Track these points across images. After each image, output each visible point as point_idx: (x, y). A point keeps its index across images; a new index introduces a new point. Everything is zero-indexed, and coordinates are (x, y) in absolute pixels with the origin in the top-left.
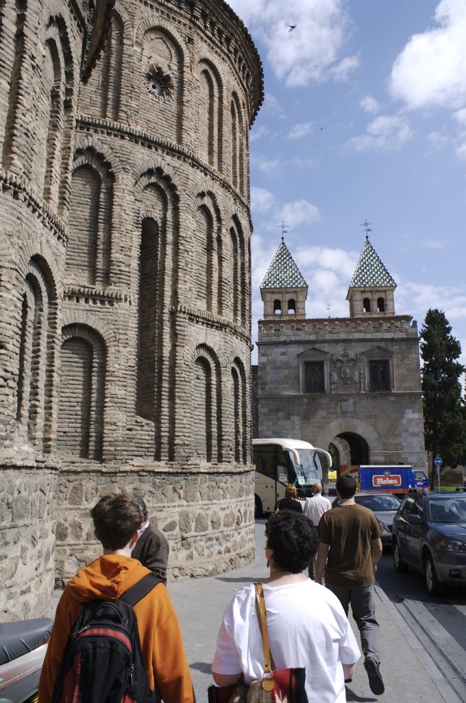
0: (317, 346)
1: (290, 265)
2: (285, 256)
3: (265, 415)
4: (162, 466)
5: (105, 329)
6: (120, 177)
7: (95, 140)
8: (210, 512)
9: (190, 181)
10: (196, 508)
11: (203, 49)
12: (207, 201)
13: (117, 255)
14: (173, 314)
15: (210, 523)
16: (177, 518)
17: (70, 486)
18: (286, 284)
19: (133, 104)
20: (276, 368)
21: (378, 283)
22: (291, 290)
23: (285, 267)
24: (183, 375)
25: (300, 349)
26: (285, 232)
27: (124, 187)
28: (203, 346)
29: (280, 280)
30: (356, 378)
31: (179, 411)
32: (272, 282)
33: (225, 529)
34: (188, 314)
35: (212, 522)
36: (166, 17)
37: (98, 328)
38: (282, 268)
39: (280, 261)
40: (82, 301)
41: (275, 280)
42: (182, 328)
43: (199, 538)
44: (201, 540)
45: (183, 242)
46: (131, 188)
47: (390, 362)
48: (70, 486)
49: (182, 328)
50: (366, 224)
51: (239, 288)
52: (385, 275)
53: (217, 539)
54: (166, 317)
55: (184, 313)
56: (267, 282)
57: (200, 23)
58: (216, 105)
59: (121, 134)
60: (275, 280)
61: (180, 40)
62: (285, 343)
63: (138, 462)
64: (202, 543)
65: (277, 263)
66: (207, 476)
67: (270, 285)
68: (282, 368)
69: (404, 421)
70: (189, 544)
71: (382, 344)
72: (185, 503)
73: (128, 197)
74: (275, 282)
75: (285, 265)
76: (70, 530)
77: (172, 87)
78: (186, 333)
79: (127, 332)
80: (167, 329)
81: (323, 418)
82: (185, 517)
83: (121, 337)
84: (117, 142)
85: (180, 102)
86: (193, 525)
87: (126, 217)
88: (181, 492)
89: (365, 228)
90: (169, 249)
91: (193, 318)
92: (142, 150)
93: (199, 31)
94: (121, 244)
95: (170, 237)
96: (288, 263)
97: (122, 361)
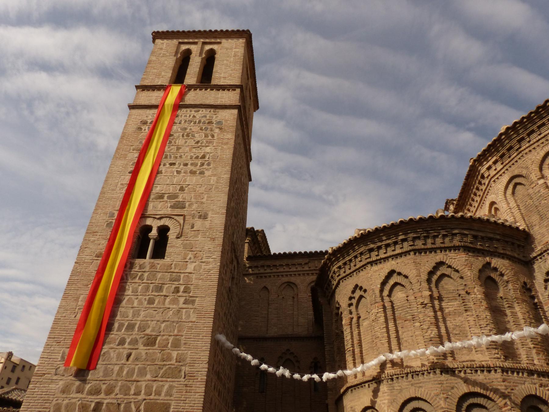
36: (547, 143)
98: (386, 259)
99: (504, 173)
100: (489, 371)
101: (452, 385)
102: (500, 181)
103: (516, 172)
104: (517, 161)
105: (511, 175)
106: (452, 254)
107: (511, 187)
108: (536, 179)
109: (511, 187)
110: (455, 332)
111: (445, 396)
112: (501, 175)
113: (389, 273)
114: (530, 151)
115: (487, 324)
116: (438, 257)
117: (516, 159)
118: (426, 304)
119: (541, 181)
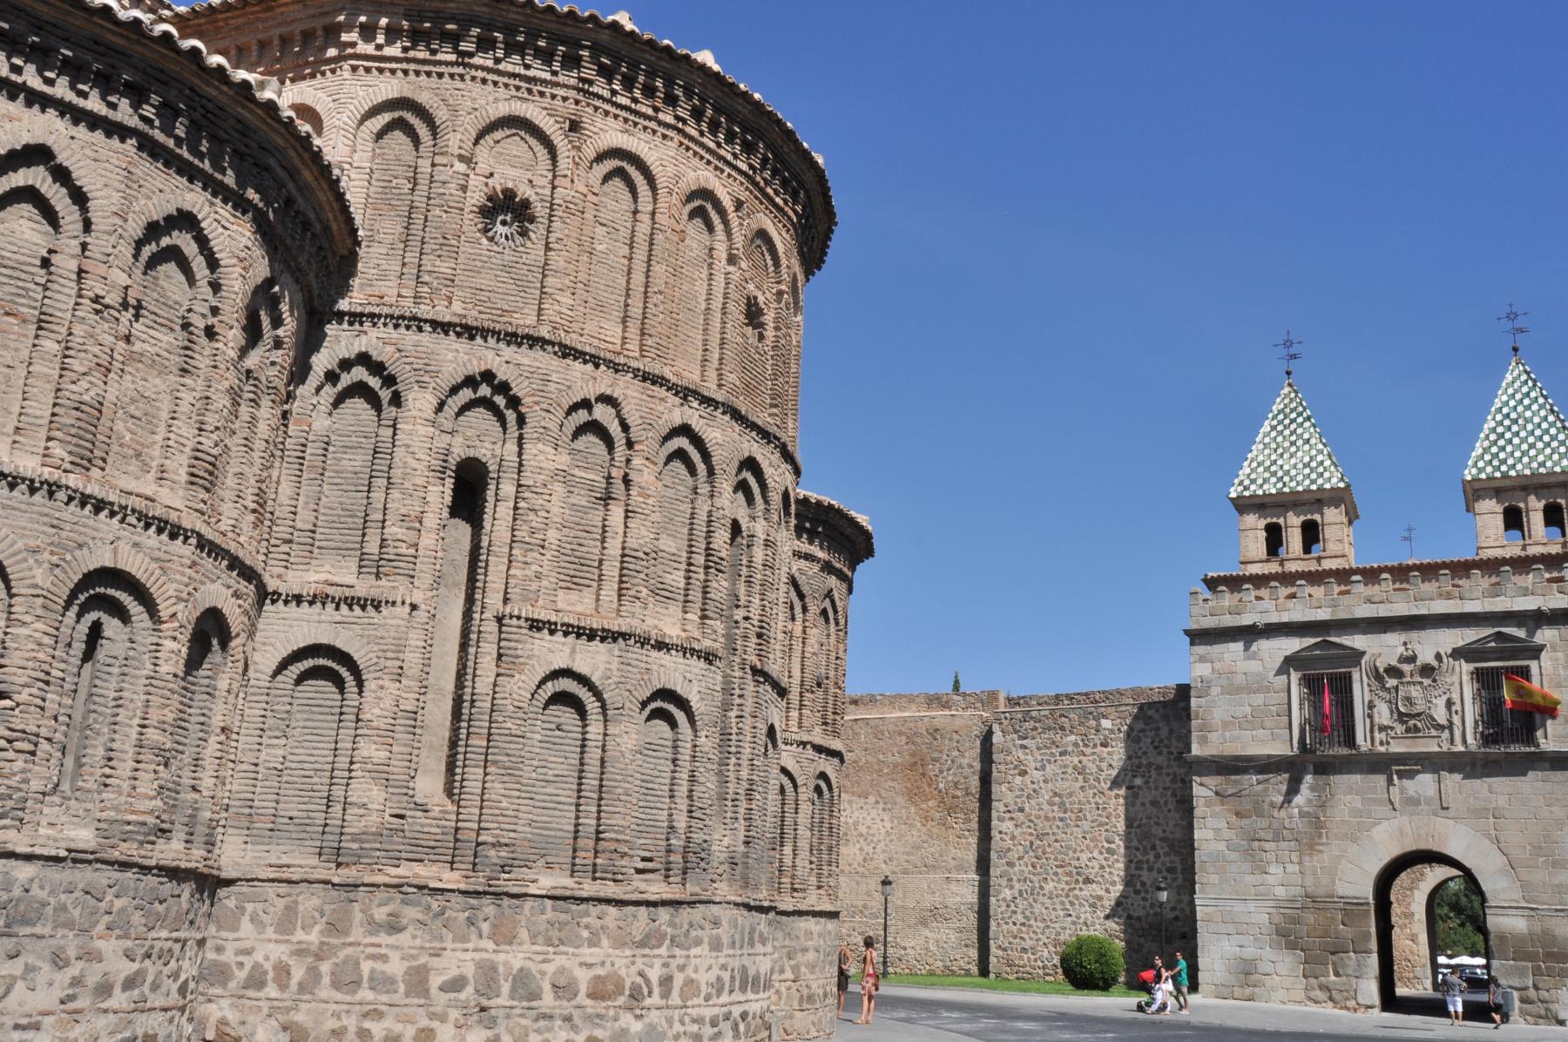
1: (1306, 436)
2: (1293, 415)
4: (451, 879)
5: (363, 652)
6: (410, 398)
7: (371, 340)
8: (550, 969)
10: (514, 958)
11: (609, 133)
12: (602, 413)
13: (394, 529)
15: (547, 987)
16: (469, 971)
17: (281, 903)
18: (1293, 484)
19: (444, 267)
21: (1543, 464)
22: (1306, 497)
23: (1293, 443)
24: (509, 725)
25: (1293, 645)
26: (1293, 357)
27: (414, 413)
29: (1280, 474)
30: (1441, 716)
31: (496, 788)
32: (1260, 481)
33: (589, 1002)
34: (527, 619)
35: (554, 986)
36: (526, 95)
37: (352, 652)
38: (1287, 444)
39: (1280, 428)
40: (330, 607)
41: (1267, 475)
42: (512, 644)
43: (518, 1011)
44: (521, 1016)
45: (527, 495)
46: (430, 414)
48: (281, 903)
49: (512, 644)
51: (700, 559)
53: (568, 1019)
54: (491, 627)
55: (519, 618)
56: (1247, 482)
57: (601, 87)
58: (644, 227)
59: (416, 322)
60: (1267, 475)
63: (405, 870)
64: (524, 1022)
65: (1273, 434)
66: (549, 903)
67: (1253, 487)
68: (1249, 690)
70: (494, 1020)
72: (491, 945)
73: (422, 430)
74: (1265, 481)
75: (1293, 438)
76: (271, 975)
77: (532, 220)
78: (519, 652)
79: (401, 656)
81: (1355, 813)
82: (488, 974)
83: (389, 663)
84: (410, 338)
85: (548, 248)
86: (506, 988)
87: (414, 464)
88: (485, 927)
89: (1508, 325)
91: (535, 625)
92: (455, 346)
93: (598, 103)
94: (404, 511)
95: (508, 489)
96: (1299, 431)
97: (388, 703)
98: (37, 100)
99: (393, 72)
100: (173, 536)
101: (81, 539)
102: (369, 79)
103: (424, 98)
104: (440, 75)
105: (407, 94)
106: (225, 211)
107: (386, 117)
108: (457, 152)
109: (386, 117)
110: (132, 409)
111: (55, 559)
112: (381, 71)
113: (27, 147)
114: (484, 81)
115: (217, 428)
116: (189, 196)
117: (442, 69)
118: (107, 307)
119: (461, 167)
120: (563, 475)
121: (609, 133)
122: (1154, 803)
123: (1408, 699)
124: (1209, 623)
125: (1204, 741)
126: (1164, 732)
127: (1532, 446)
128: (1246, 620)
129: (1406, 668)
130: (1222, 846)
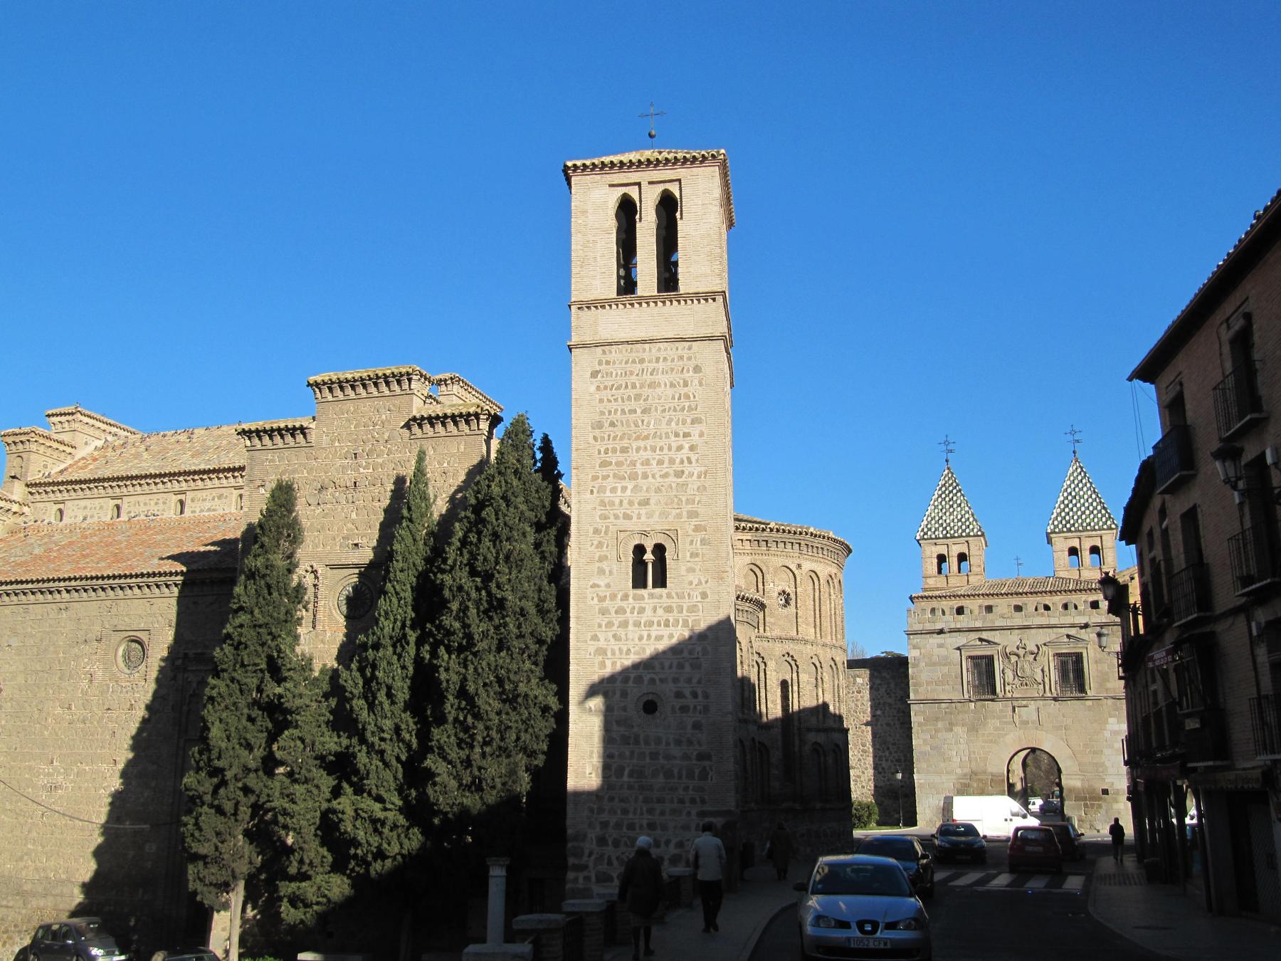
0: (985, 635)
3: (920, 724)
9: (803, 653)
11: (807, 565)
12: (815, 660)
14: (799, 729)
20: (932, 664)
25: (961, 640)
28: (816, 743)
30: (1039, 677)
47: (1085, 655)
50: (1073, 433)
52: (1100, 512)
61: (794, 569)
62: (941, 632)
68: (939, 664)
69: (1107, 734)
71: (1072, 632)
80: (796, 738)
81: (996, 729)
89: (1070, 438)
90: (796, 695)
91: (809, 730)
95: (795, 688)
120: (808, 682)
121: (807, 565)
122: (888, 725)
123: (1022, 668)
124: (918, 627)
125: (916, 692)
126: (892, 685)
127: (1084, 513)
128: (939, 626)
129: (1021, 652)
130: (928, 748)
